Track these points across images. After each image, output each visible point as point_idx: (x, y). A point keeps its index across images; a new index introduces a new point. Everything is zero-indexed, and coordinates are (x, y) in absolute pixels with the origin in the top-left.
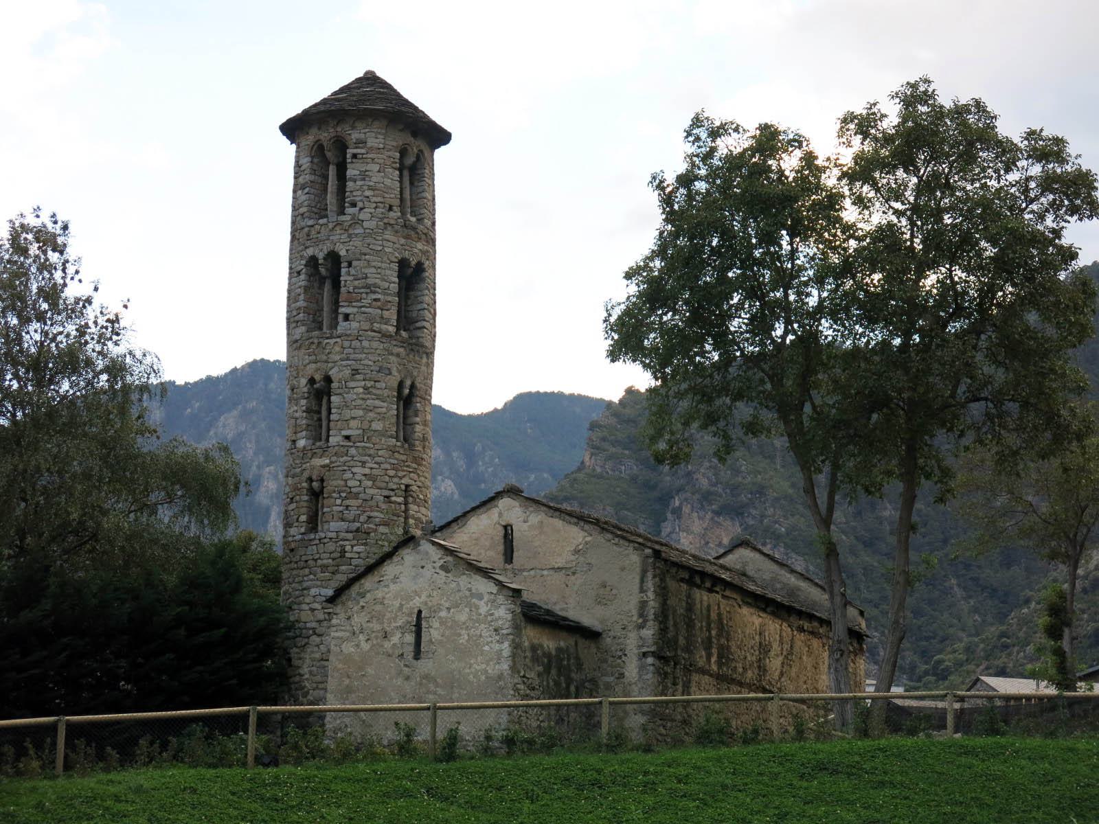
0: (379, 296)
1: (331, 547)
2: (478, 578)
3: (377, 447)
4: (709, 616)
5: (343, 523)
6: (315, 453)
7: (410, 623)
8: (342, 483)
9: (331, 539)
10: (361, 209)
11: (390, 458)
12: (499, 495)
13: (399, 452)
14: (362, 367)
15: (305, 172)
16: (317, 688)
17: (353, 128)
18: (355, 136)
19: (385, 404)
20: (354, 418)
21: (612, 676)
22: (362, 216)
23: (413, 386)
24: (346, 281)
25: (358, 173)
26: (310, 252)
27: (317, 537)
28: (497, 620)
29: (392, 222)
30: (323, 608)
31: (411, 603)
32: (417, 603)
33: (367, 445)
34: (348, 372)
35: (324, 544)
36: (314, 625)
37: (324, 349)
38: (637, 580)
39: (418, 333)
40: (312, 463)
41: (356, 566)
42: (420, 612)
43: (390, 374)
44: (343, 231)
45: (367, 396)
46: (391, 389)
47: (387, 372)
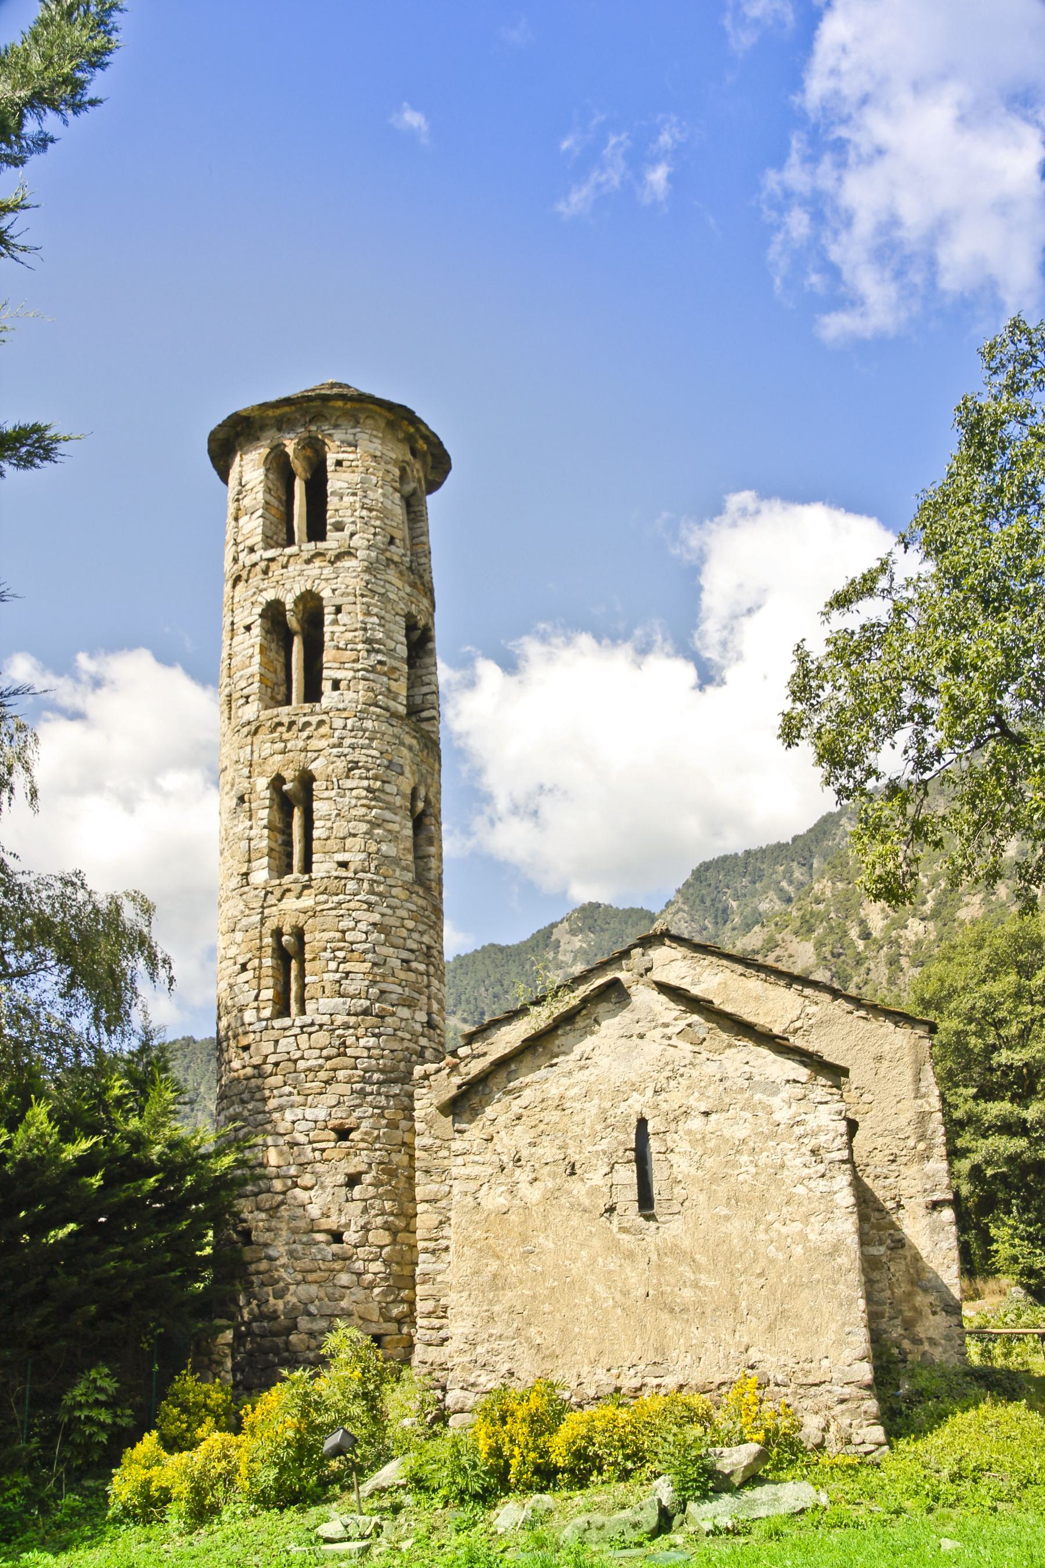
0: (384, 659)
1: (321, 1038)
3: (390, 881)
6: (289, 890)
7: (623, 1143)
8: (338, 935)
9: (321, 1026)
10: (352, 535)
11: (406, 901)
13: (417, 894)
15: (255, 490)
16: (305, 1281)
17: (336, 426)
19: (397, 818)
21: (881, 1244)
23: (427, 801)
24: (333, 633)
25: (346, 485)
26: (270, 595)
27: (298, 1023)
28: (814, 1134)
29: (396, 559)
32: (637, 1104)
34: (341, 765)
38: (908, 1076)
41: (366, 1072)
42: (642, 1123)
43: (402, 774)
45: (373, 803)
46: (404, 796)
47: (399, 770)
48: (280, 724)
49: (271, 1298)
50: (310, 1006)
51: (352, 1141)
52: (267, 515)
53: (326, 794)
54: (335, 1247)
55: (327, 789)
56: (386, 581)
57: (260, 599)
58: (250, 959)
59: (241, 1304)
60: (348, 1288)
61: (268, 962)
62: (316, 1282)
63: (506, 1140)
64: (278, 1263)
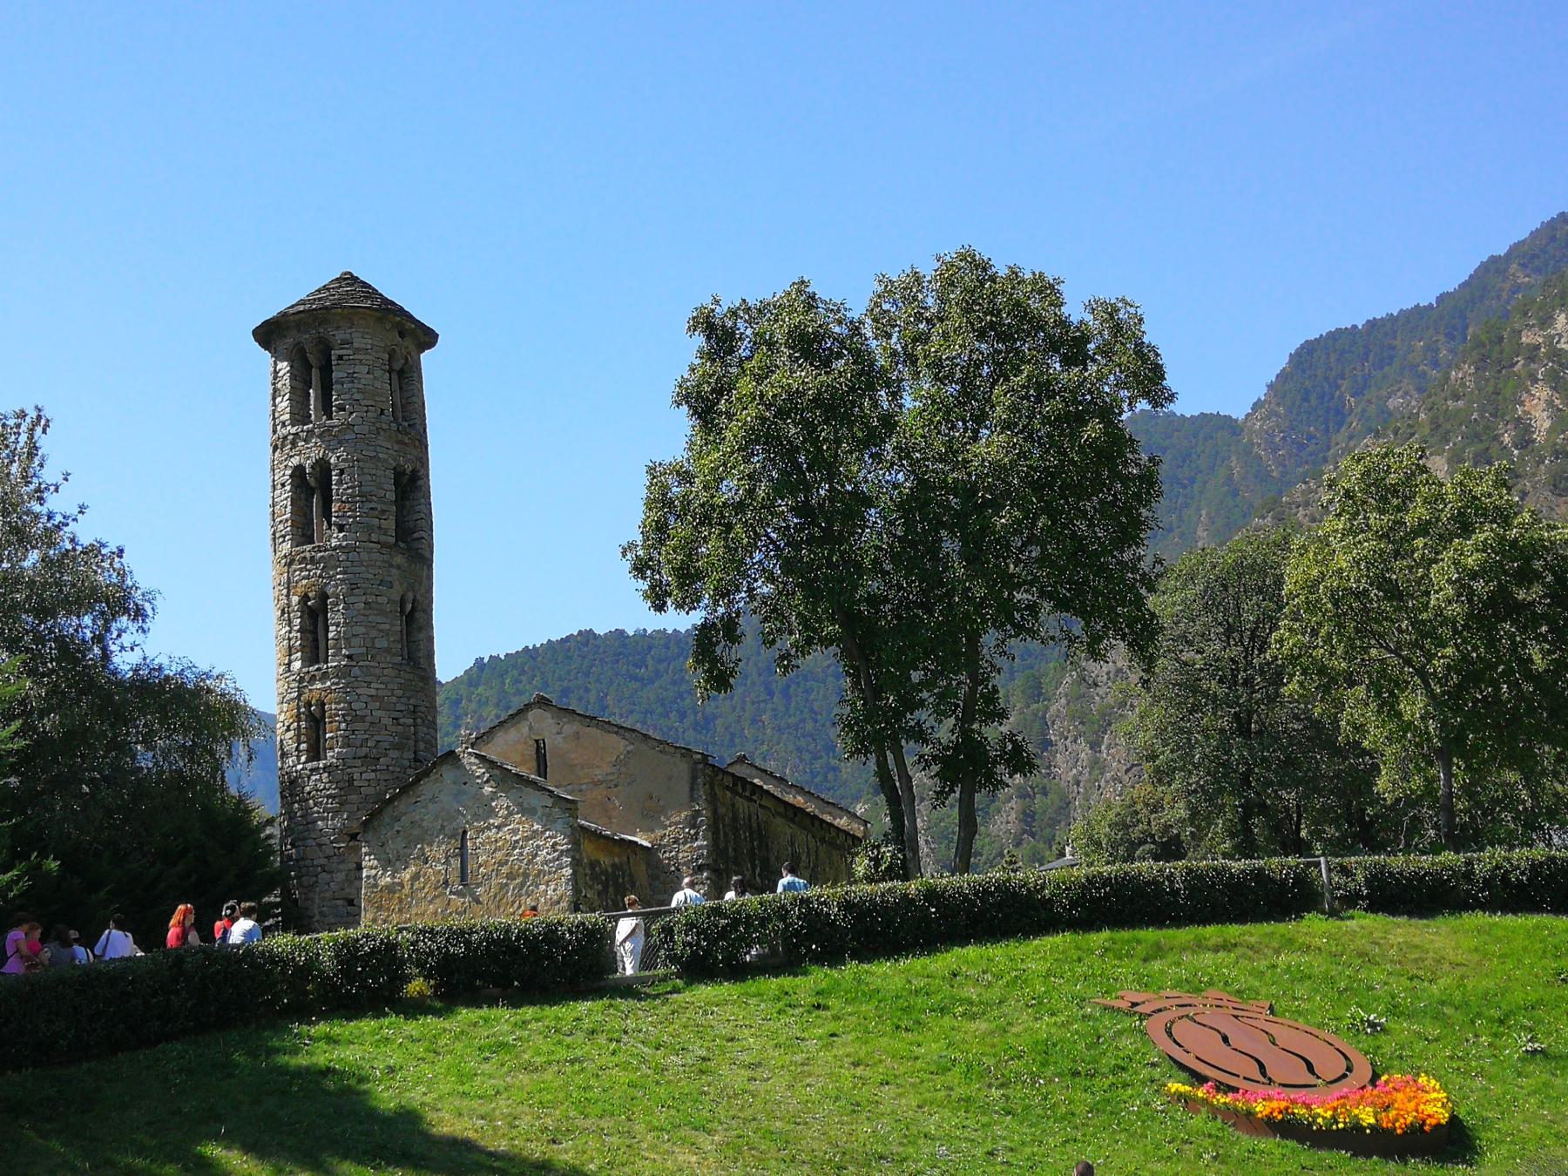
2: (529, 790)
4: (751, 827)
12: (528, 707)
17: (338, 328)
18: (340, 335)
26: (295, 461)
31: (454, 824)
33: (372, 664)
36: (323, 861)
38: (687, 789)
39: (416, 545)
45: (367, 613)
52: (294, 397)
54: (349, 908)
56: (376, 446)
57: (290, 464)
61: (303, 724)
63: (392, 846)
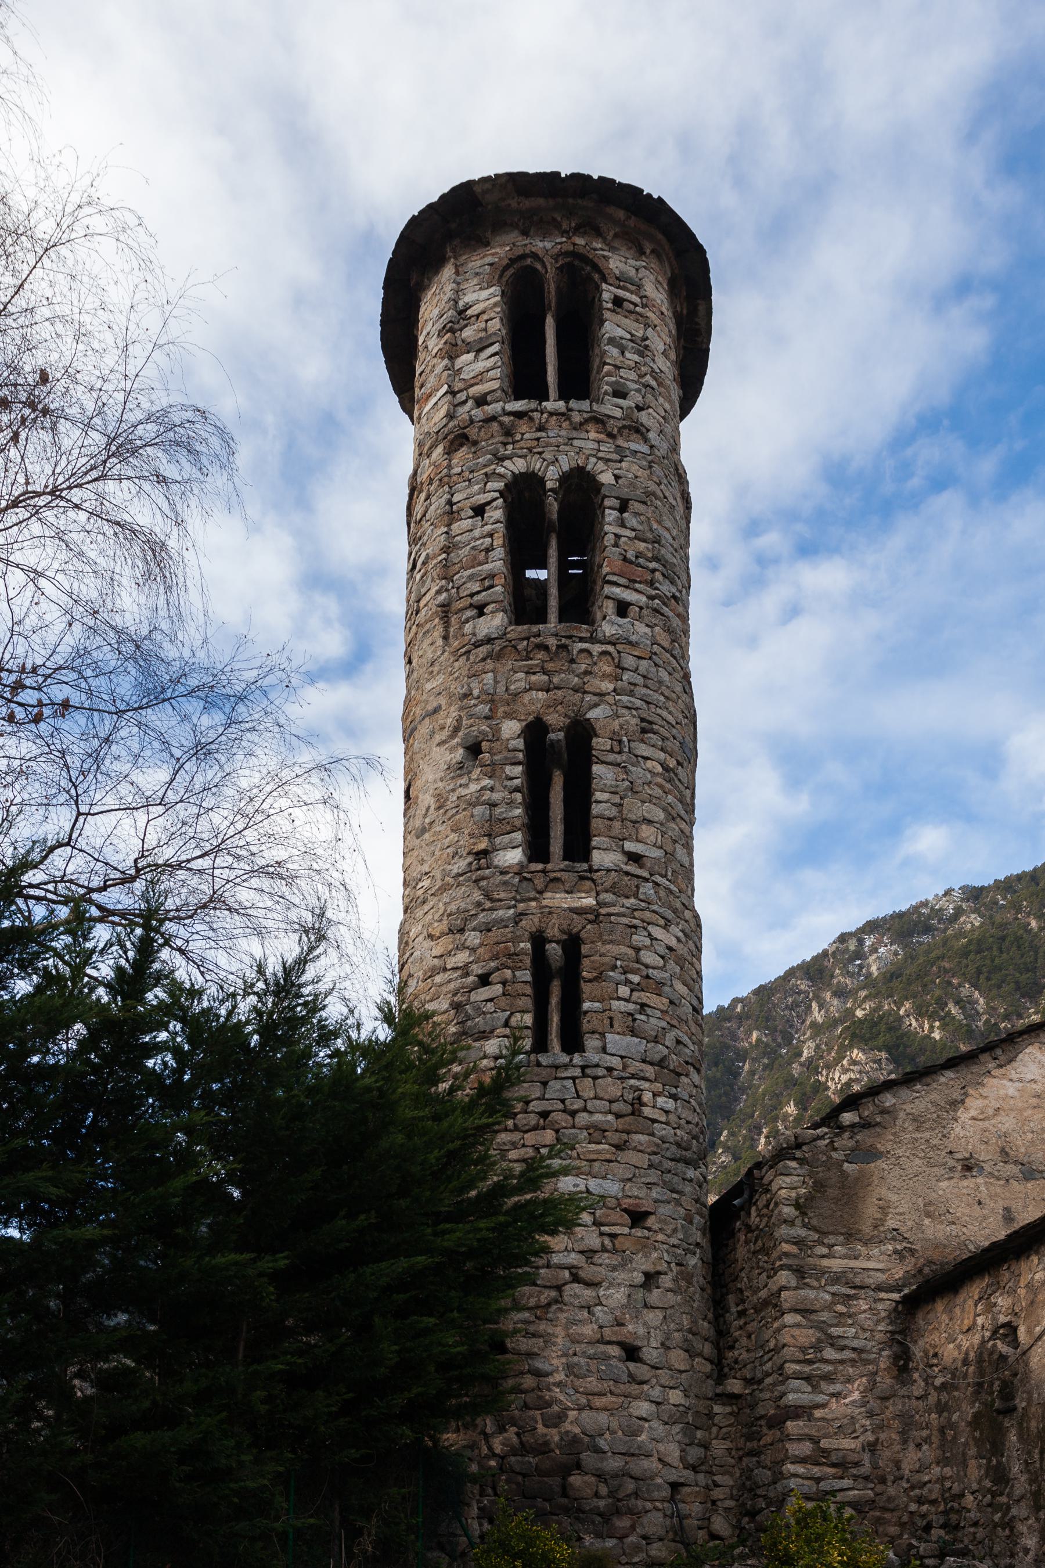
1: (611, 1088)
5: (634, 1039)
8: (631, 952)
9: (610, 1070)
14: (657, 719)
20: (650, 822)
22: (643, 417)
26: (518, 465)
30: (594, 1224)
34: (633, 722)
35: (595, 1078)
36: (573, 1258)
37: (572, 661)
40: (545, 903)
44: (602, 437)
48: (546, 648)
49: (540, 1426)
50: (592, 1043)
51: (649, 1229)
53: (611, 757)
54: (631, 1365)
55: (612, 751)
57: (501, 470)
58: (498, 969)
59: (488, 1430)
60: (646, 1420)
62: (606, 1409)
64: (551, 1379)
